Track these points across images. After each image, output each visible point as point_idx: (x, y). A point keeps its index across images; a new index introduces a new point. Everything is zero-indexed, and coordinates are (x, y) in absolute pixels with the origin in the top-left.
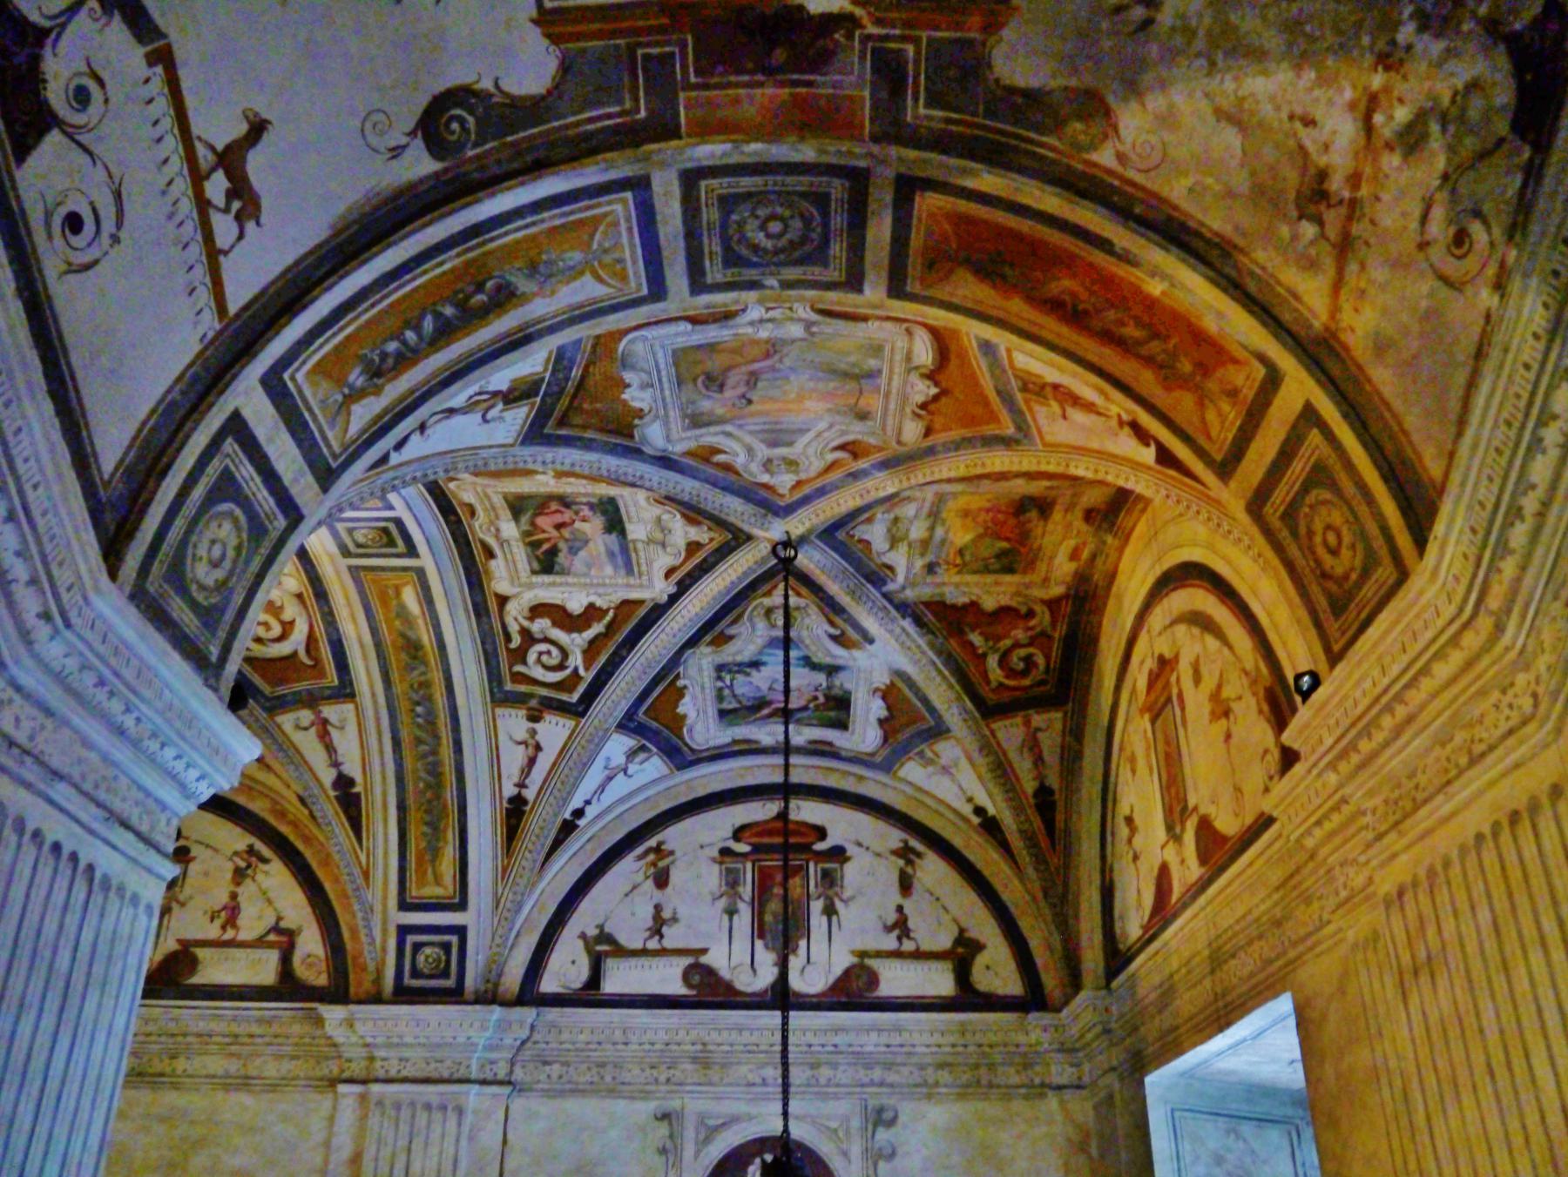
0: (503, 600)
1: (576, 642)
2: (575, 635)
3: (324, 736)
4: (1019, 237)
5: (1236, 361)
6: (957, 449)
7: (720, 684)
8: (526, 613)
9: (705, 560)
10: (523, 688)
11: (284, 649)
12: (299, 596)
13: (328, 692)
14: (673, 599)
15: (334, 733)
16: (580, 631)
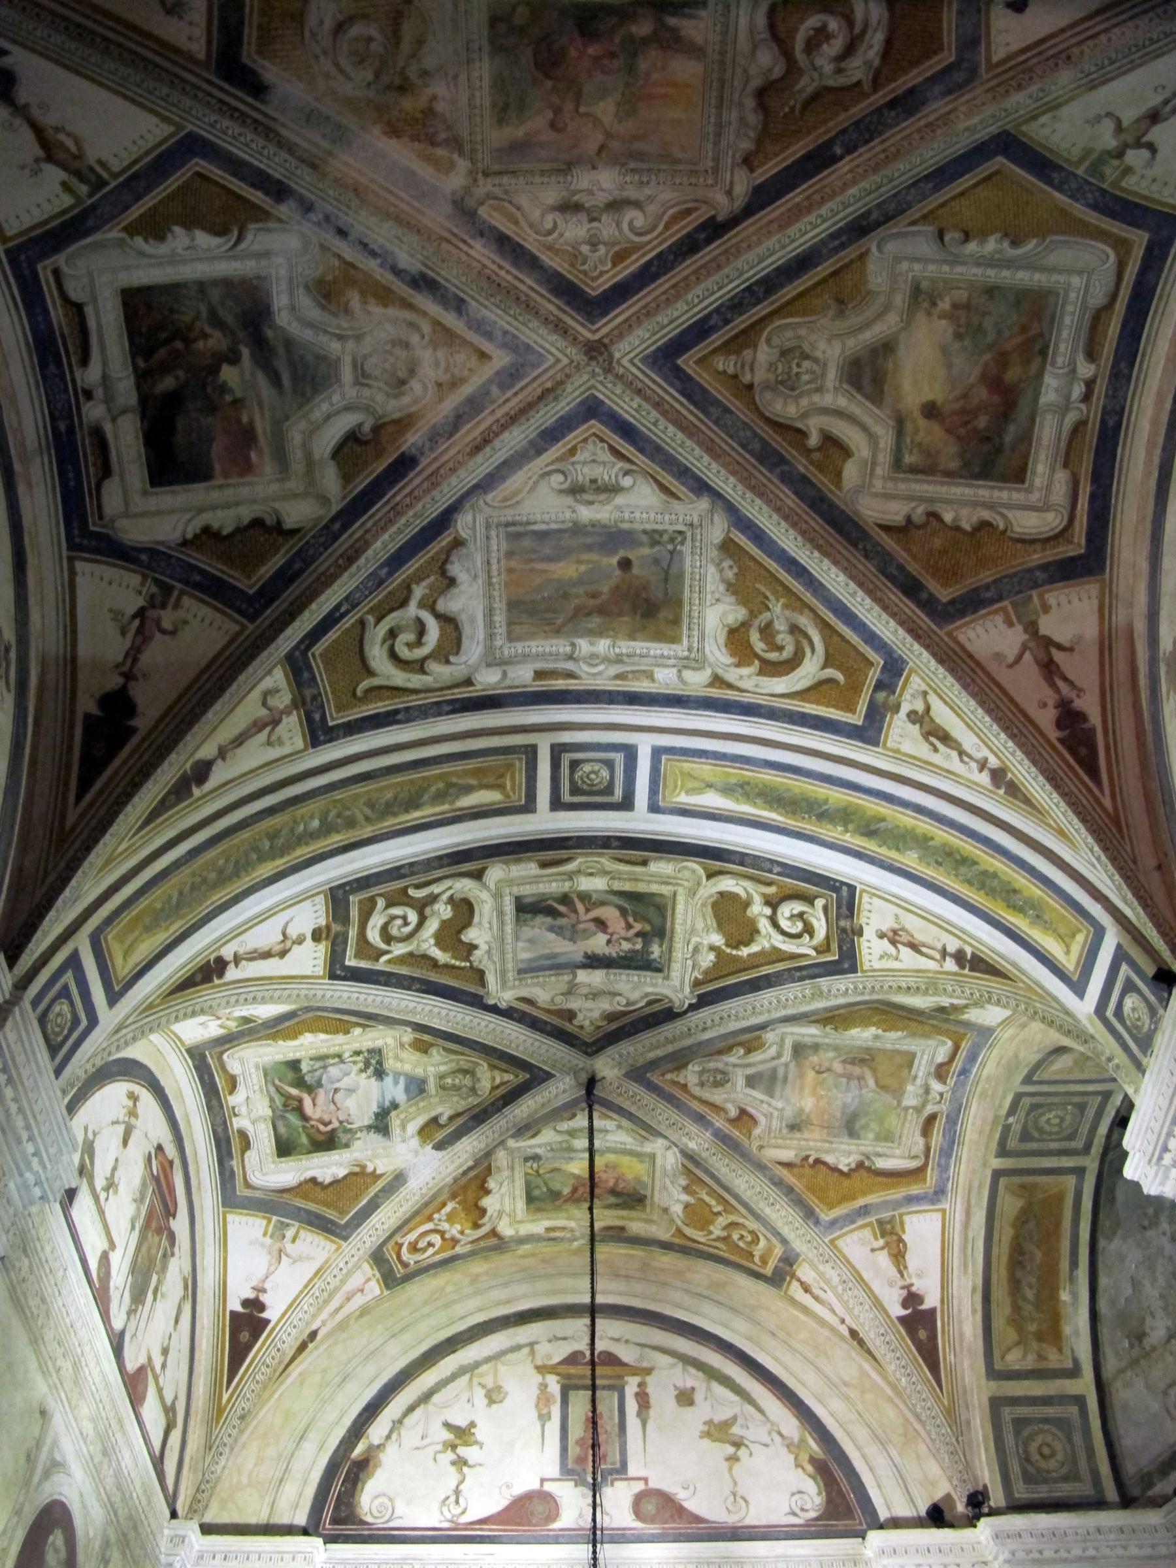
0: (478, 875)
1: (426, 943)
2: (432, 941)
3: (258, 726)
4: (1058, 1225)
5: (1060, 1350)
6: (775, 1184)
7: (347, 1055)
8: (458, 896)
9: (546, 1023)
10: (354, 913)
11: (377, 655)
12: (468, 682)
13: (317, 717)
14: (494, 1009)
15: (263, 736)
16: (437, 944)
